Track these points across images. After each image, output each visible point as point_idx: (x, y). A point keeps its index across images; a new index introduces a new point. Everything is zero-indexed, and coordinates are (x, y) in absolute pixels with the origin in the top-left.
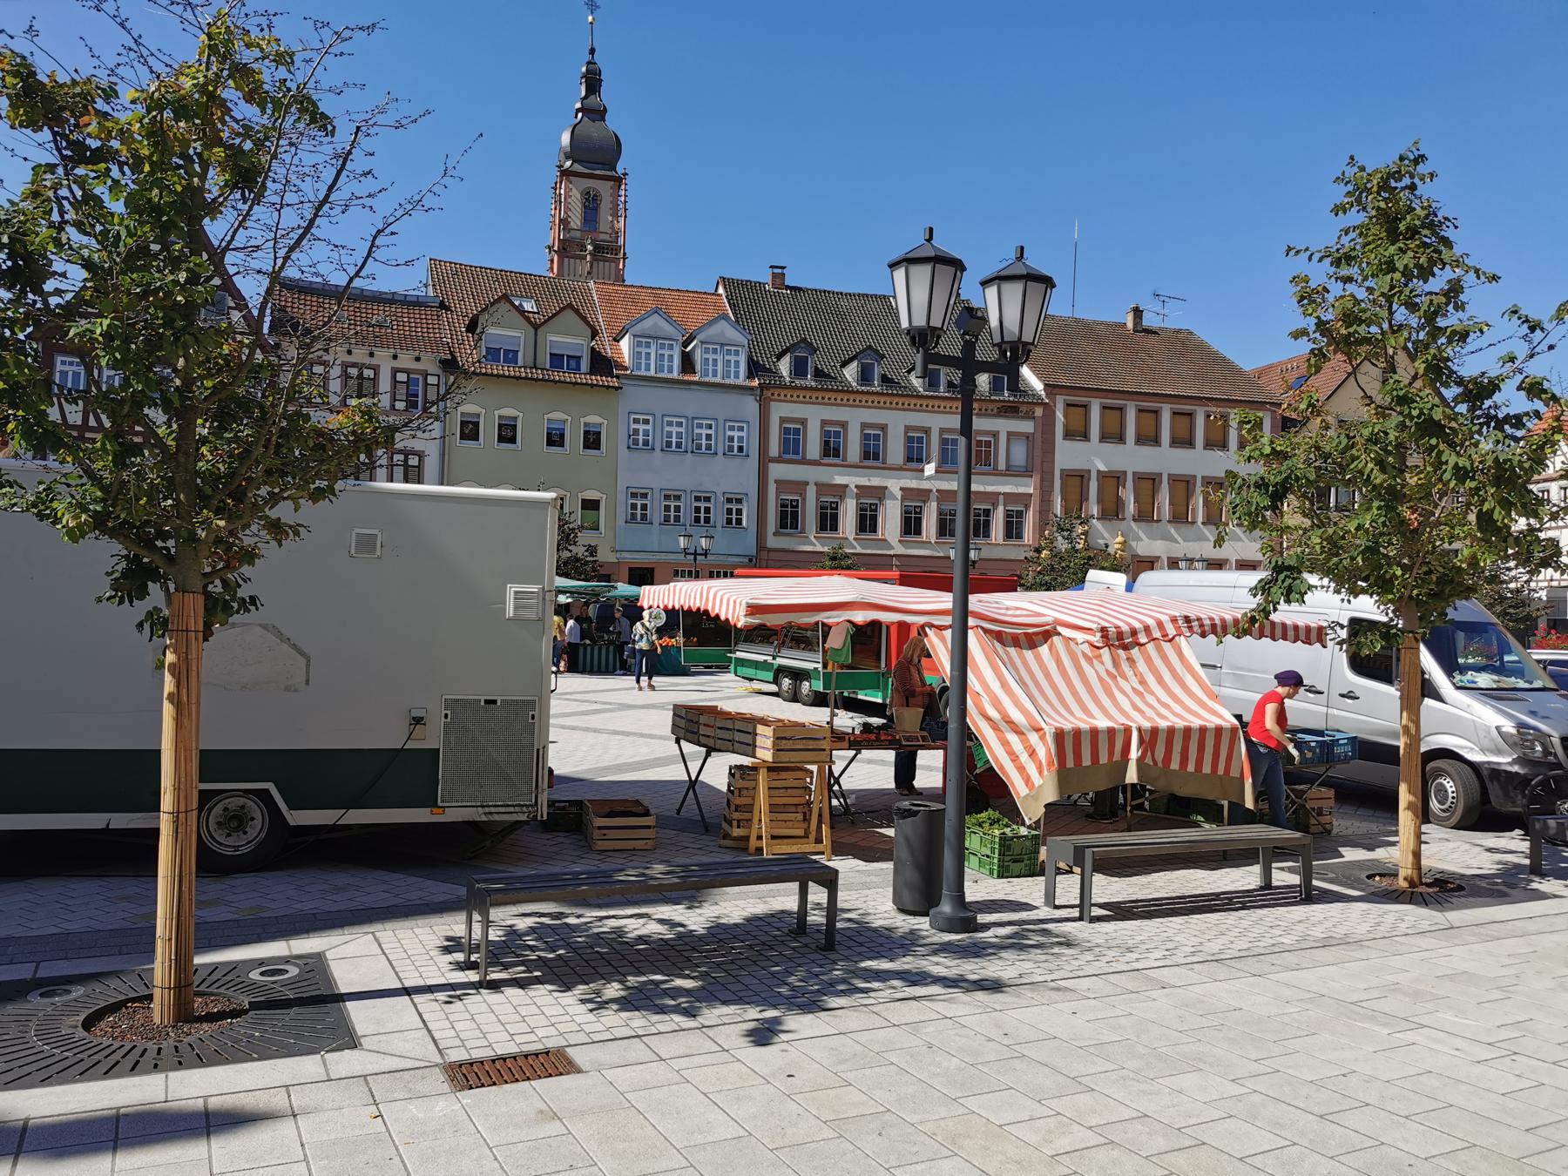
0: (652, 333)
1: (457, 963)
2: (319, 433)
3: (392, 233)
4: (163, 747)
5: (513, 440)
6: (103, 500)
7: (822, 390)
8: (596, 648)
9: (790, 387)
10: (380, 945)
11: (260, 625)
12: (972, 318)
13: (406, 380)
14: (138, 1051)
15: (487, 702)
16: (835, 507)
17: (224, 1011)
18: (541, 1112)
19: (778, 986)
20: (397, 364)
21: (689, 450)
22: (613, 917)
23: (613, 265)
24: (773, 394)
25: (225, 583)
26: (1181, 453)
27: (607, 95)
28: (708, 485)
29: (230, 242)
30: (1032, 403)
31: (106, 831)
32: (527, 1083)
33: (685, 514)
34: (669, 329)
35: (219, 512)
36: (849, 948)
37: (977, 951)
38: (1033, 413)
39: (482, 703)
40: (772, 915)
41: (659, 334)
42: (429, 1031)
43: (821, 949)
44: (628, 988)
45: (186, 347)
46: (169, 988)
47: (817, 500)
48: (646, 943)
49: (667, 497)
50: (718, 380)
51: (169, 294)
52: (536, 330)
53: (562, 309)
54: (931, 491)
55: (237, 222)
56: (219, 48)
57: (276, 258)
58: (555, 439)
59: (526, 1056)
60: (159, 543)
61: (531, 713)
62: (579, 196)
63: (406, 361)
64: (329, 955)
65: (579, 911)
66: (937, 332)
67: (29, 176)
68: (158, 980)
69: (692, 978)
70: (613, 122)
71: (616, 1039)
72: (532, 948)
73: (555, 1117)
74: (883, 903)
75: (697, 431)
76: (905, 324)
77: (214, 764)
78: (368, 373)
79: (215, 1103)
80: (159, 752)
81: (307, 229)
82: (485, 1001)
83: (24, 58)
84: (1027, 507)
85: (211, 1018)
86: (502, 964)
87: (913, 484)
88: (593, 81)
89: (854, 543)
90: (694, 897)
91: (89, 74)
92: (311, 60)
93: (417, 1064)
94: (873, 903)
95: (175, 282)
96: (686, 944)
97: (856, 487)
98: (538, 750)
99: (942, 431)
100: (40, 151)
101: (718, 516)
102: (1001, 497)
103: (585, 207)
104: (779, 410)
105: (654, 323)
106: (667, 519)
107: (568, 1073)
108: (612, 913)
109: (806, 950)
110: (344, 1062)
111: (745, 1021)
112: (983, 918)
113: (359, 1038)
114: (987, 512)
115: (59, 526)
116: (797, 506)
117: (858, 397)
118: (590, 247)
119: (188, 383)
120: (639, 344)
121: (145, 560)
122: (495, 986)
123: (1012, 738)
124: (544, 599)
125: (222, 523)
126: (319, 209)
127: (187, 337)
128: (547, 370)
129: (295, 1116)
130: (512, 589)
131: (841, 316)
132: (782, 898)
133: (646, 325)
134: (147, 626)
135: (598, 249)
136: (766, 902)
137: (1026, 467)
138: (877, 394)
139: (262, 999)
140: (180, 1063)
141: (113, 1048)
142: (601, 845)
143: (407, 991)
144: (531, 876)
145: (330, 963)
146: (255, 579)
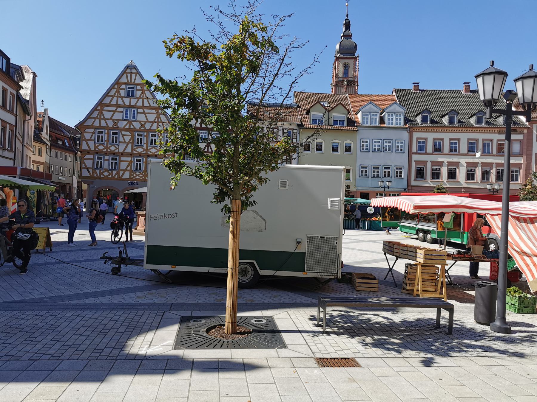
0: (370, 111)
1: (315, 324)
2: (274, 149)
3: (297, 82)
4: (229, 247)
5: (321, 150)
6: (214, 172)
7: (434, 127)
8: (350, 220)
9: (421, 127)
10: (289, 316)
11: (252, 211)
12: (511, 95)
14: (222, 341)
15: (321, 237)
16: (438, 170)
17: (245, 332)
18: (349, 379)
19: (431, 346)
21: (382, 151)
22: (366, 314)
23: (354, 88)
24: (414, 130)
25: (246, 197)
27: (352, 30)
28: (389, 163)
29: (249, 90)
30: (524, 128)
31: (208, 273)
32: (343, 368)
33: (380, 173)
34: (375, 109)
35: (246, 174)
36: (458, 335)
37: (512, 341)
38: (523, 131)
39: (320, 238)
40: (425, 320)
41: (372, 111)
42: (309, 346)
43: (447, 334)
44: (374, 340)
45: (238, 124)
46: (230, 323)
47: (431, 167)
48: (379, 324)
49: (374, 168)
50: (393, 126)
51: (233, 107)
53: (337, 105)
54: (478, 163)
55: (251, 83)
56: (245, 29)
57: (263, 94)
58: (335, 149)
59: (342, 359)
60: (228, 185)
61: (336, 242)
62: (342, 66)
63: (287, 125)
64: (275, 317)
65: (354, 311)
66: (496, 101)
67: (193, 75)
68: (226, 320)
69: (397, 339)
70: (354, 39)
71: (372, 357)
72: (339, 322)
73: (355, 381)
74: (470, 319)
75: (385, 144)
76: (482, 98)
77: (243, 254)
79: (246, 361)
80: (228, 249)
81: (271, 84)
82: (325, 338)
83: (191, 39)
84: (520, 168)
85: (241, 333)
86: (329, 326)
87: (471, 160)
88: (347, 26)
89: (446, 183)
90: (395, 310)
91: (208, 42)
92: (273, 29)
93: (304, 356)
94: (465, 319)
95: (235, 103)
96: (394, 327)
97: (447, 162)
98: (338, 255)
100: (195, 67)
101: (393, 174)
103: (344, 69)
104: (416, 135)
105: (370, 107)
106: (374, 175)
107: (357, 367)
108: (365, 313)
109: (440, 334)
110: (282, 352)
111: (420, 357)
112: (513, 329)
113: (287, 345)
114: (517, 171)
115: (202, 180)
116: (423, 170)
117: (448, 129)
118: (346, 83)
119: (237, 135)
120: (364, 115)
121: (224, 190)
122: (328, 333)
123: (526, 258)
124: (341, 203)
125: (247, 178)
126: (275, 77)
127: (238, 120)
128: (333, 126)
129: (270, 368)
130: (330, 199)
131: (441, 99)
132: (430, 313)
133: (367, 108)
134: (224, 210)
135: (349, 83)
136: (422, 314)
137: (520, 153)
138: (456, 127)
139: (256, 329)
140: (234, 347)
141: (215, 340)
142: (359, 289)
143: (300, 332)
144: (339, 297)
145: (275, 320)
146: (255, 196)
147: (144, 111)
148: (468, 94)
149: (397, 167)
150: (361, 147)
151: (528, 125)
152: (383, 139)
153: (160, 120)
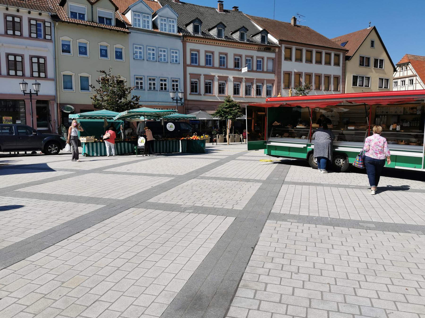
0: (141, 11)
5: (85, 53)
7: (205, 38)
9: (194, 37)
16: (210, 84)
20: (31, 16)
21: (158, 60)
24: (187, 40)
26: (318, 66)
28: (165, 75)
33: (157, 86)
34: (148, 11)
38: (275, 50)
41: (143, 11)
47: (205, 81)
49: (150, 80)
50: (167, 32)
63: (35, 14)
78: (17, 20)
84: (273, 84)
89: (218, 97)
97: (218, 76)
99: (246, 56)
101: (169, 87)
102: (265, 81)
104: (190, 46)
106: (150, 88)
116: (197, 84)
117: (218, 42)
120: (135, 15)
137: (273, 70)
148: (222, 13)
149: (173, 79)
150: (134, 54)
151: (278, 44)
152: (157, 47)
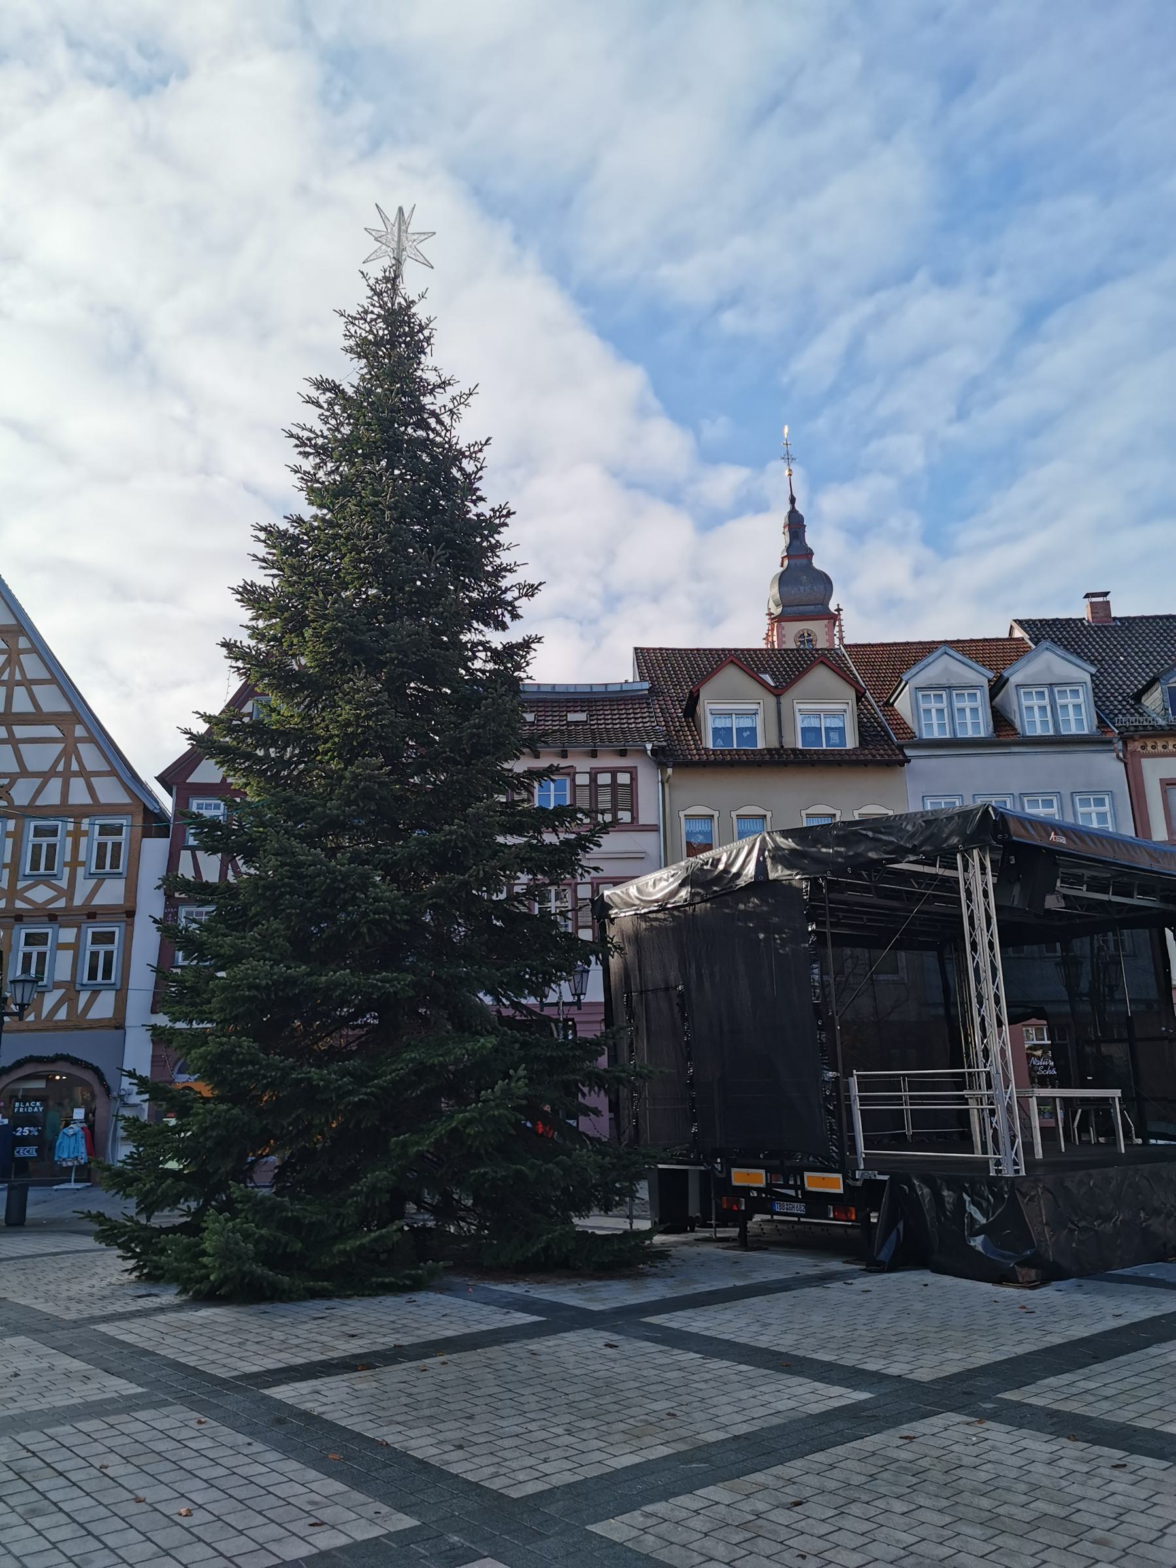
0: (944, 681)
13: (609, 782)
24: (1143, 748)
41: (954, 682)
52: (778, 696)
147: (11, 733)
152: (1016, 794)
153: (75, 767)
